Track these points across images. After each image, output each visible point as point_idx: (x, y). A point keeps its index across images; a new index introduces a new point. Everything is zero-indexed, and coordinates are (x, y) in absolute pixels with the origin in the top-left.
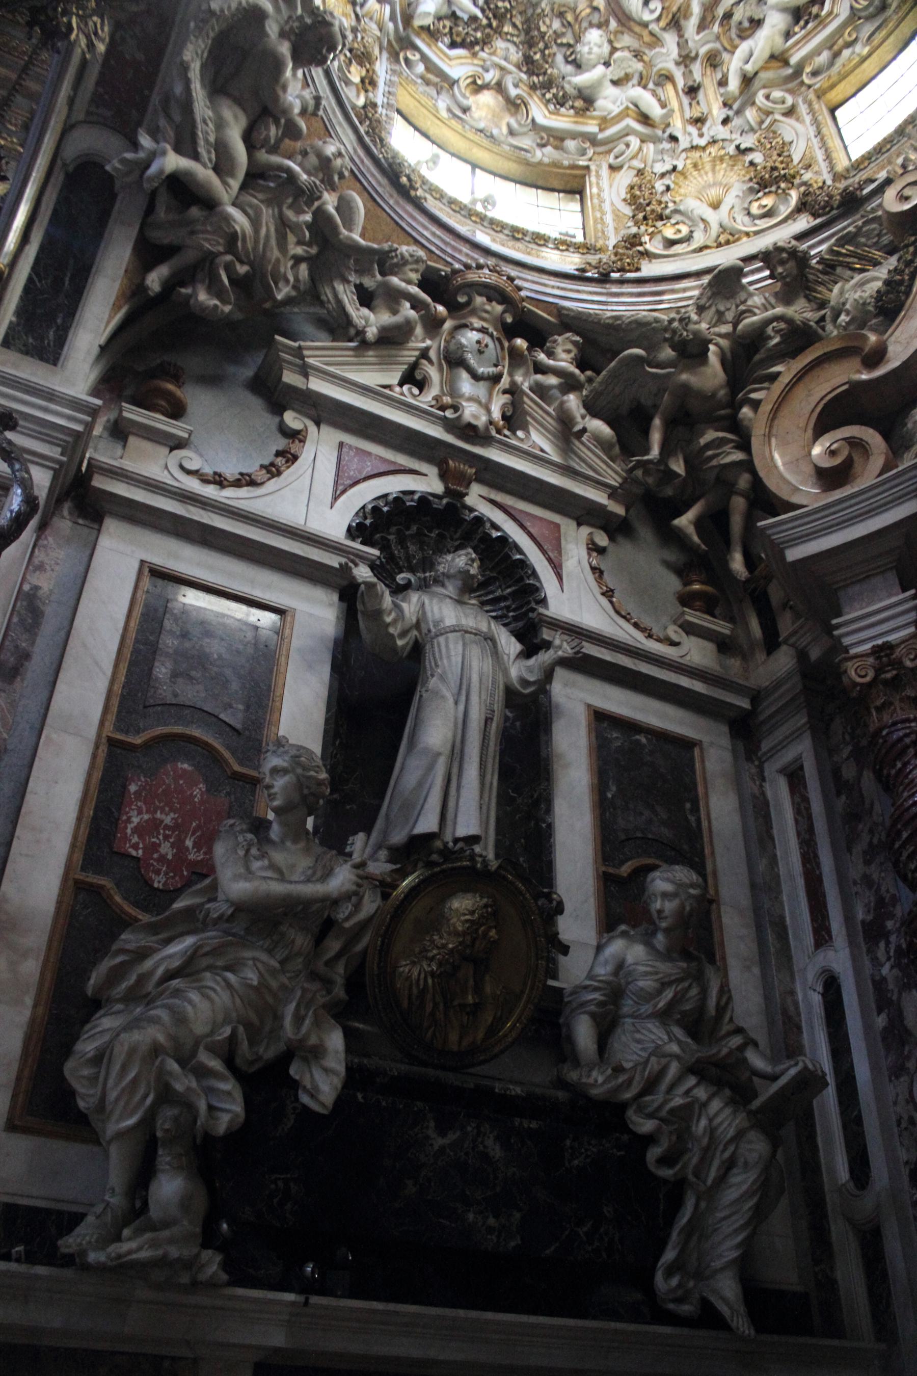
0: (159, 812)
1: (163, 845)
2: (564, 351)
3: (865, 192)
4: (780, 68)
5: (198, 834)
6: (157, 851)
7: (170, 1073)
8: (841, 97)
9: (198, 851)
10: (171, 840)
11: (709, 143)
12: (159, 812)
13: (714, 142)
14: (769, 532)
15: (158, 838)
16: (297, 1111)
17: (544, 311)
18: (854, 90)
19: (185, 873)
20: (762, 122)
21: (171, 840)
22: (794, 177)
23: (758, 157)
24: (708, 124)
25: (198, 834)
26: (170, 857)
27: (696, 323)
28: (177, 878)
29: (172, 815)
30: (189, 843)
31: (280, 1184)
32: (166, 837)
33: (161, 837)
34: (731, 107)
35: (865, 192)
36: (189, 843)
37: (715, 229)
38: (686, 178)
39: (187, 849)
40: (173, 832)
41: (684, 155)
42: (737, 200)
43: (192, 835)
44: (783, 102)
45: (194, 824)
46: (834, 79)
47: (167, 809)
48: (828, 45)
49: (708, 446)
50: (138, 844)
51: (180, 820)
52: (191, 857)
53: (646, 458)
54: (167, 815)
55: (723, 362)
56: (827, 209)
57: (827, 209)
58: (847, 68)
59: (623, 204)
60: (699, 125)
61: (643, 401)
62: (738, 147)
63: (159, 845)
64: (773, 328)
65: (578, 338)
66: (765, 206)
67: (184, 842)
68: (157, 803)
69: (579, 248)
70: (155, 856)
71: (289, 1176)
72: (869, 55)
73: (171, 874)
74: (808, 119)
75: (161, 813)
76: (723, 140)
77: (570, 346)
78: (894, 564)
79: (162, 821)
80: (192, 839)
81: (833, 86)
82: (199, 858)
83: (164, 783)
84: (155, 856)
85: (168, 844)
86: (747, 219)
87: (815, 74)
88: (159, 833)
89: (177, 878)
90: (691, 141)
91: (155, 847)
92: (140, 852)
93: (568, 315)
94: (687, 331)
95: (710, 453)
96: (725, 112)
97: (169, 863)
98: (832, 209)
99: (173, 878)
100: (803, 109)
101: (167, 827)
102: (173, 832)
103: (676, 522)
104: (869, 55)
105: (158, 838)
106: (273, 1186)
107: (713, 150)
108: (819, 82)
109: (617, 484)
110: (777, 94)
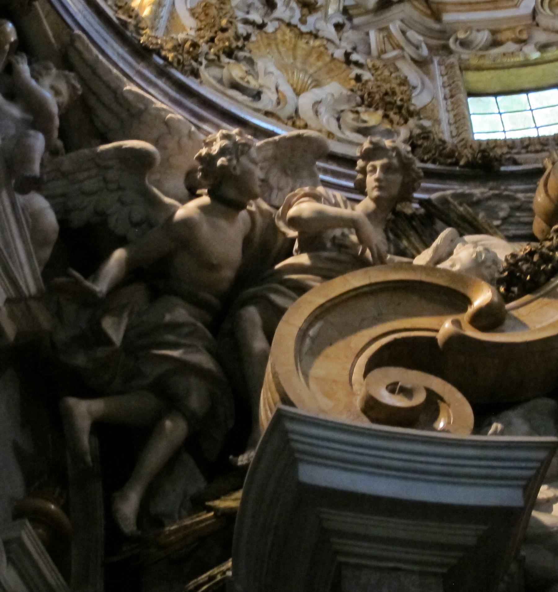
2: (52, 88)
3: (503, 169)
4: (426, 15)
8: (480, 86)
11: (310, 33)
13: (315, 36)
14: (289, 425)
17: (52, 29)
18: (498, 89)
20: (384, 52)
22: (411, 114)
23: (367, 76)
24: (319, 15)
27: (254, 162)
34: (350, 19)
35: (503, 169)
37: (288, 110)
38: (269, 45)
41: (276, 24)
42: (329, 98)
44: (417, 47)
46: (486, 62)
48: (492, 27)
49: (174, 327)
53: (88, 283)
55: (247, 241)
56: (449, 161)
57: (449, 161)
58: (505, 60)
59: (187, 14)
60: (306, 11)
61: (112, 222)
62: (347, 55)
64: (334, 238)
65: (78, 86)
66: (365, 122)
69: (120, 8)
72: (536, 63)
74: (439, 81)
76: (329, 40)
77: (63, 87)
78: (445, 570)
81: (479, 69)
86: (334, 123)
87: (464, 44)
90: (292, 17)
93: (80, 53)
94: (238, 161)
95: (171, 338)
96: (340, 19)
98: (456, 163)
100: (436, 68)
103: (72, 401)
104: (536, 63)
107: (313, 43)
108: (465, 54)
109: (27, 293)
110: (413, 35)
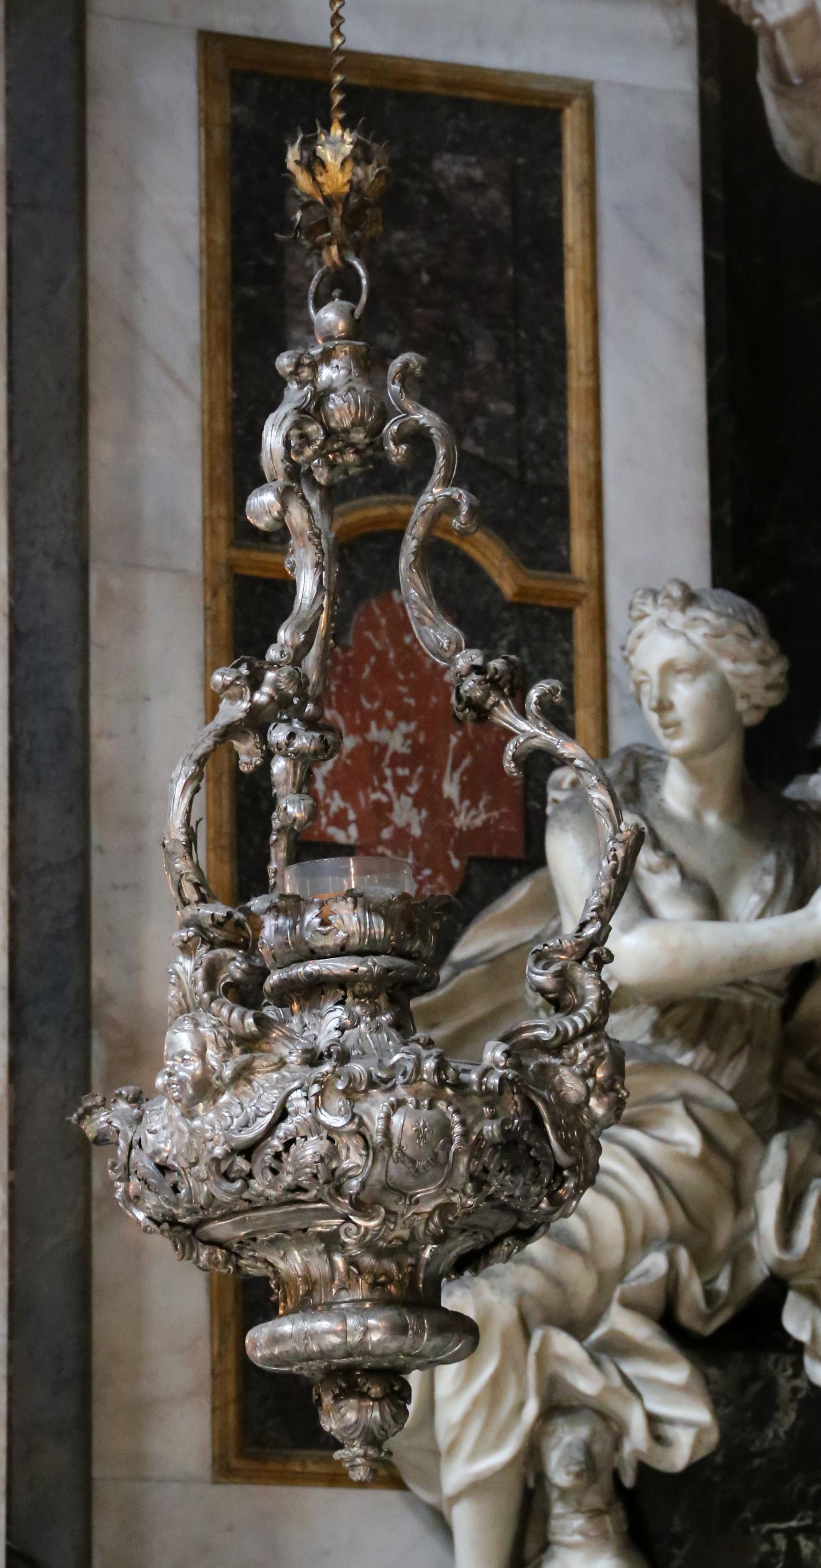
0: (373, 725)
1: (396, 806)
5: (466, 762)
6: (389, 823)
7: (563, 1360)
9: (474, 805)
10: (413, 789)
12: (373, 725)
15: (384, 791)
16: (800, 1396)
19: (456, 863)
21: (413, 789)
25: (466, 762)
26: (416, 831)
28: (440, 879)
29: (403, 727)
30: (451, 789)
31: (781, 1543)
32: (401, 785)
33: (389, 786)
36: (451, 789)
39: (449, 803)
40: (412, 771)
43: (454, 768)
45: (454, 740)
47: (389, 714)
50: (343, 812)
51: (422, 739)
52: (462, 821)
54: (392, 728)
63: (390, 807)
67: (439, 790)
68: (367, 705)
70: (386, 834)
71: (793, 1524)
73: (427, 872)
75: (379, 728)
79: (384, 748)
80: (457, 776)
82: (478, 822)
83: (373, 651)
84: (386, 834)
85: (407, 801)
88: (383, 779)
89: (440, 879)
91: (382, 811)
92: (353, 830)
97: (417, 844)
99: (431, 879)
101: (397, 760)
102: (412, 771)
105: (384, 791)
106: (765, 1547)
